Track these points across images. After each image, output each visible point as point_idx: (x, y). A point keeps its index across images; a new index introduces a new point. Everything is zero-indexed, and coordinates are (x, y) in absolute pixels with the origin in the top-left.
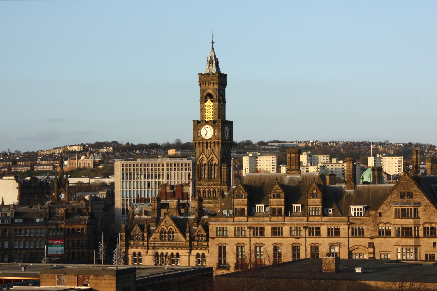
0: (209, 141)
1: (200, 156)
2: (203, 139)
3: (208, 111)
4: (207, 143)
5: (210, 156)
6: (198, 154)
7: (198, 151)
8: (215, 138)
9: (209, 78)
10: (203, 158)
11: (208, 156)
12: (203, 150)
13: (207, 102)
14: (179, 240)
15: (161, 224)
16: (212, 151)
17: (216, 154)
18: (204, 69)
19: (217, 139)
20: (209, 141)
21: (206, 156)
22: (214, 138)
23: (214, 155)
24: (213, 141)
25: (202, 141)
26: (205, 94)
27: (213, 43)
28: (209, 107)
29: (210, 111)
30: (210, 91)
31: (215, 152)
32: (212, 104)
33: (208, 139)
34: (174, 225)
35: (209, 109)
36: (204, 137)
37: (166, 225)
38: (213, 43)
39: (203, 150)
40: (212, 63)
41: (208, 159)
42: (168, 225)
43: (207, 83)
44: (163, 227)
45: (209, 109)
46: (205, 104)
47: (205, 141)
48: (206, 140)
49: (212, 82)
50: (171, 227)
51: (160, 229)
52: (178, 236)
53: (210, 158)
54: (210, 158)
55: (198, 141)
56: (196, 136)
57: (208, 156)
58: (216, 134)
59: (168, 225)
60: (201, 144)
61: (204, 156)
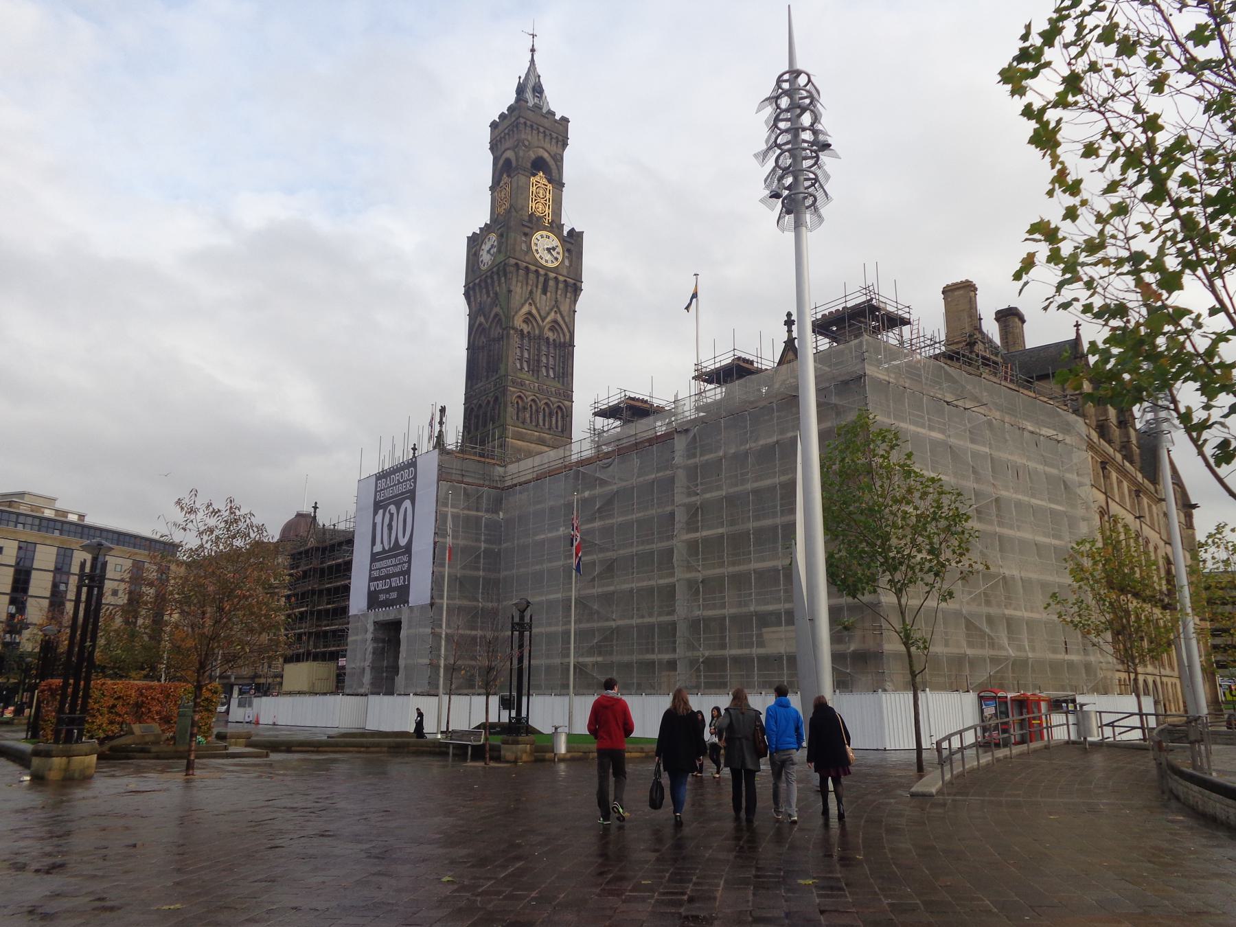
0: (552, 275)
1: (523, 305)
2: (536, 263)
5: (548, 314)
6: (517, 297)
7: (519, 290)
10: (530, 313)
12: (531, 292)
13: (537, 178)
17: (565, 314)
20: (552, 275)
26: (533, 156)
27: (533, 50)
30: (546, 155)
31: (562, 309)
32: (550, 187)
36: (538, 256)
38: (533, 50)
39: (531, 292)
49: (554, 135)
53: (549, 319)
57: (543, 313)
58: (567, 263)
60: (532, 276)
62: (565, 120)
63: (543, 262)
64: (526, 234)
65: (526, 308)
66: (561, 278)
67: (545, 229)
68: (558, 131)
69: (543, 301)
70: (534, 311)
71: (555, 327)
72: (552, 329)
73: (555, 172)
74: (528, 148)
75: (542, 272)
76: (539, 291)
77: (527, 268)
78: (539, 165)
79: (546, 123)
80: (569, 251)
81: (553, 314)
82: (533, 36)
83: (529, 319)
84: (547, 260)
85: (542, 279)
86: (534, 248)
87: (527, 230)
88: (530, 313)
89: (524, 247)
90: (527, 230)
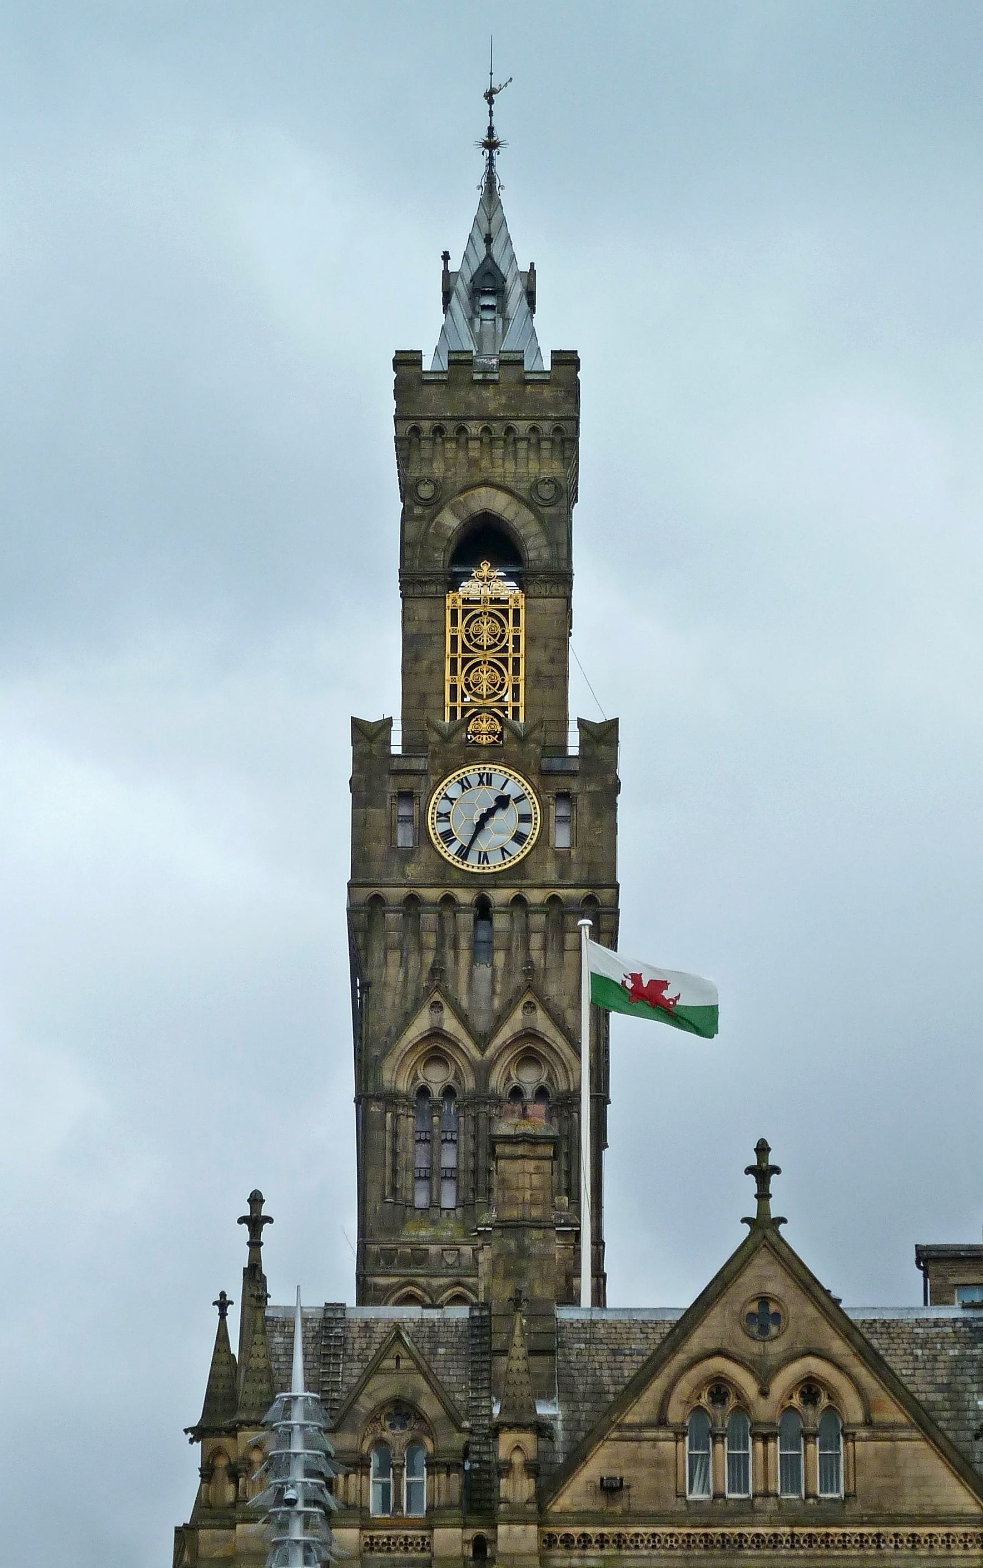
0: (500, 896)
1: (407, 1018)
2: (444, 873)
3: (479, 655)
4: (483, 910)
5: (500, 1019)
7: (394, 974)
8: (562, 876)
9: (488, 393)
10: (436, 1033)
11: (482, 1022)
12: (437, 971)
13: (470, 589)
14: (908, 1505)
15: (697, 1342)
16: (518, 979)
18: (425, 330)
19: (576, 874)
21: (463, 1018)
22: (550, 872)
23: (540, 1014)
24: (536, 896)
25: (433, 894)
26: (450, 521)
27: (491, 145)
28: (485, 628)
29: (491, 656)
30: (499, 503)
33: (497, 880)
34: (838, 1346)
35: (485, 640)
36: (449, 852)
37: (756, 1348)
39: (433, 971)
40: (500, 291)
41: (482, 1041)
42: (776, 1348)
43: (474, 428)
44: (718, 1364)
45: (485, 640)
46: (452, 600)
47: (465, 896)
48: (470, 880)
49: (522, 427)
50: (814, 1365)
51: (684, 1387)
52: (890, 1464)
53: (506, 1033)
54: (506, 1033)
55: (404, 891)
56: (379, 849)
58: (562, 838)
59: (776, 1348)
60: (429, 919)
61: (450, 1024)
62: (567, 361)
63: (472, 865)
64: (406, 796)
65: (422, 1023)
66: (536, 896)
67: (471, 753)
68: (548, 404)
69: (477, 982)
70: (450, 1024)
71: (529, 1049)
72: (529, 1058)
73: (535, 549)
74: (435, 504)
75: (465, 896)
76: (465, 956)
77: (412, 900)
78: (487, 541)
79: (493, 401)
80: (564, 797)
81: (518, 1014)
82: (490, 96)
83: (436, 1048)
84: (500, 845)
85: (466, 919)
86: (436, 828)
87: (407, 783)
88: (436, 1033)
89: (404, 837)
90: (407, 783)
